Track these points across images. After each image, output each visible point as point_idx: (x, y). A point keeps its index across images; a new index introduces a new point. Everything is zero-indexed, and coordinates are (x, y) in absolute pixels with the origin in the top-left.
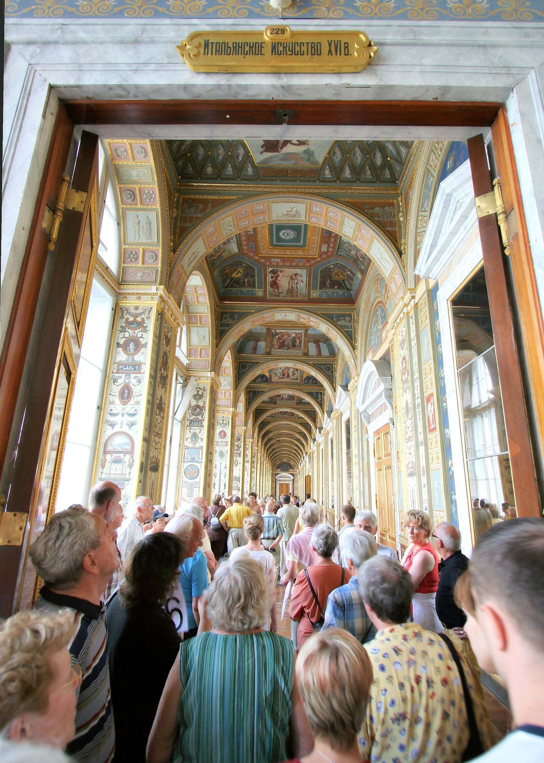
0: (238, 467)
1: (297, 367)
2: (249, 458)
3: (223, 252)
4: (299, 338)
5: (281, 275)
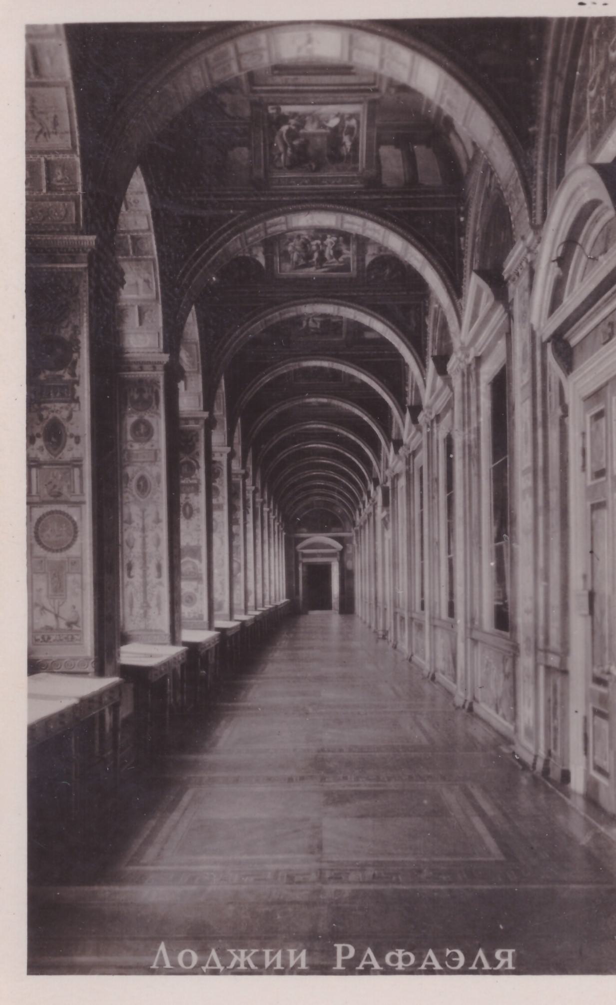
0: (194, 521)
1: (347, 227)
2: (222, 498)
4: (351, 131)
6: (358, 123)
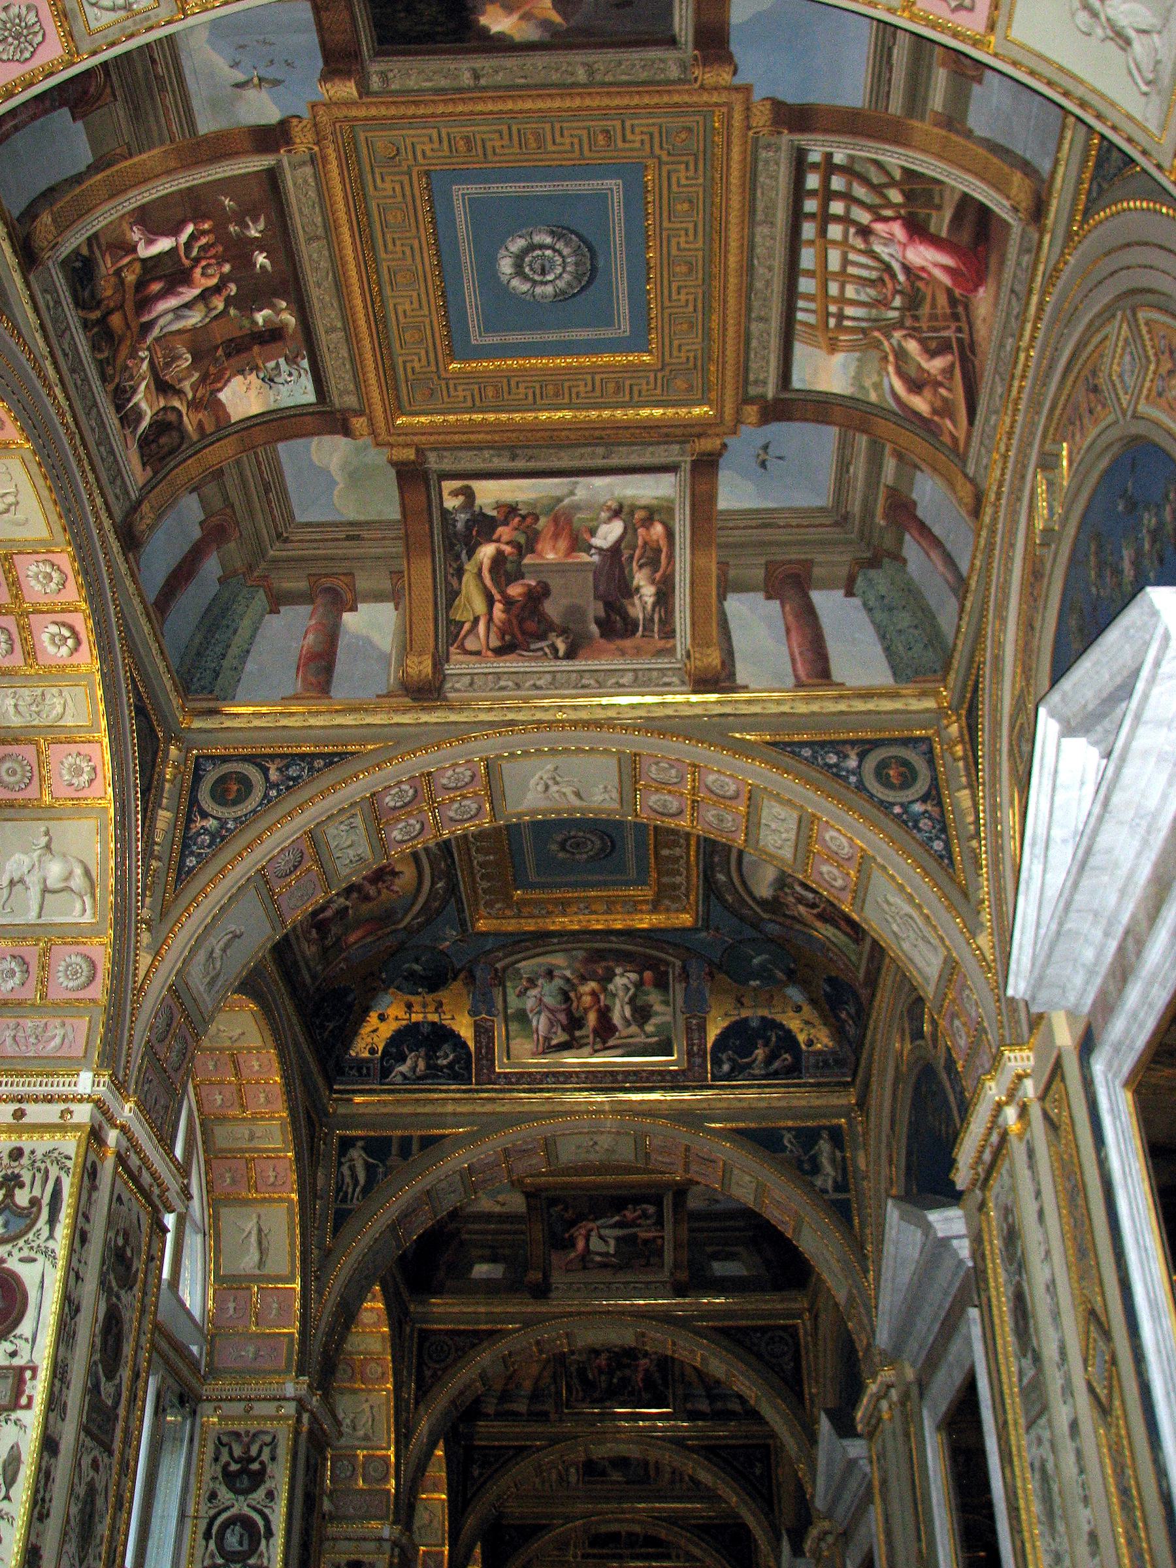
6: (670, 534)
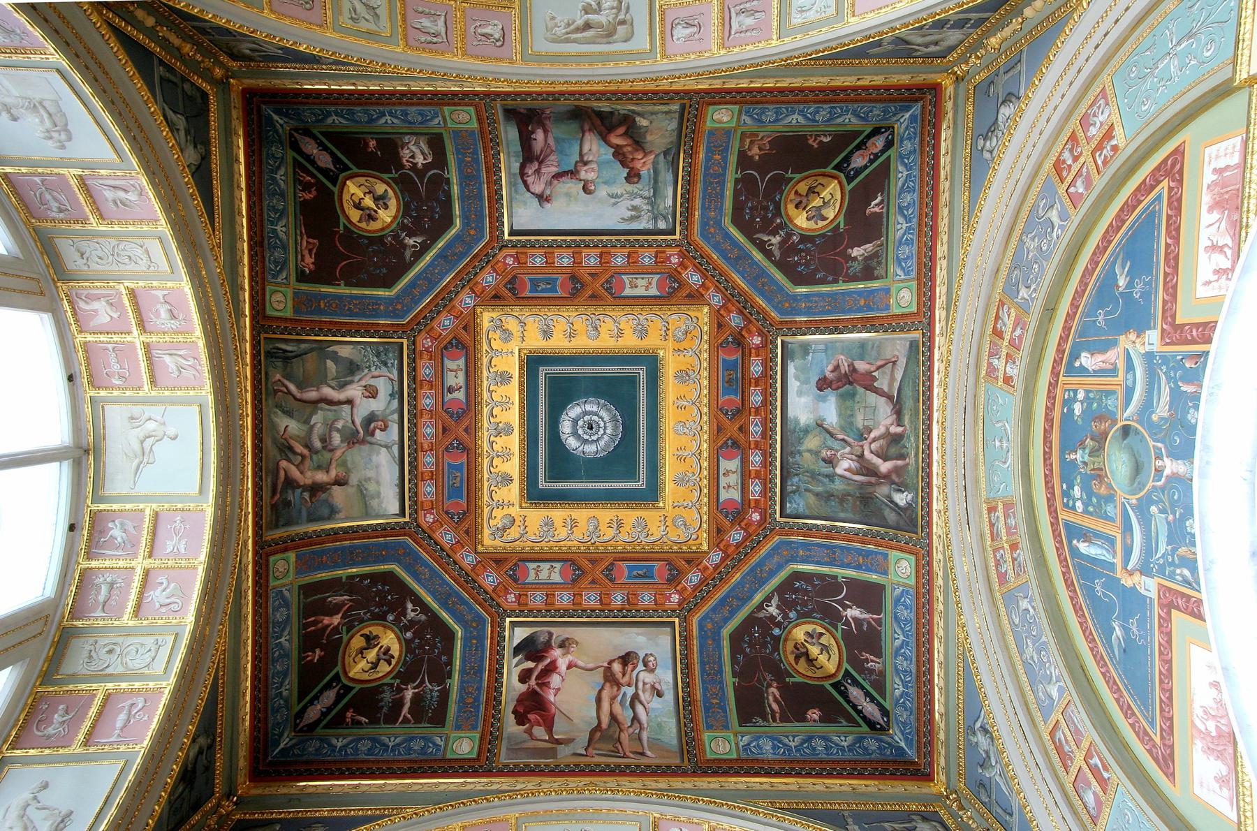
3: (340, 482)
5: (562, 664)
